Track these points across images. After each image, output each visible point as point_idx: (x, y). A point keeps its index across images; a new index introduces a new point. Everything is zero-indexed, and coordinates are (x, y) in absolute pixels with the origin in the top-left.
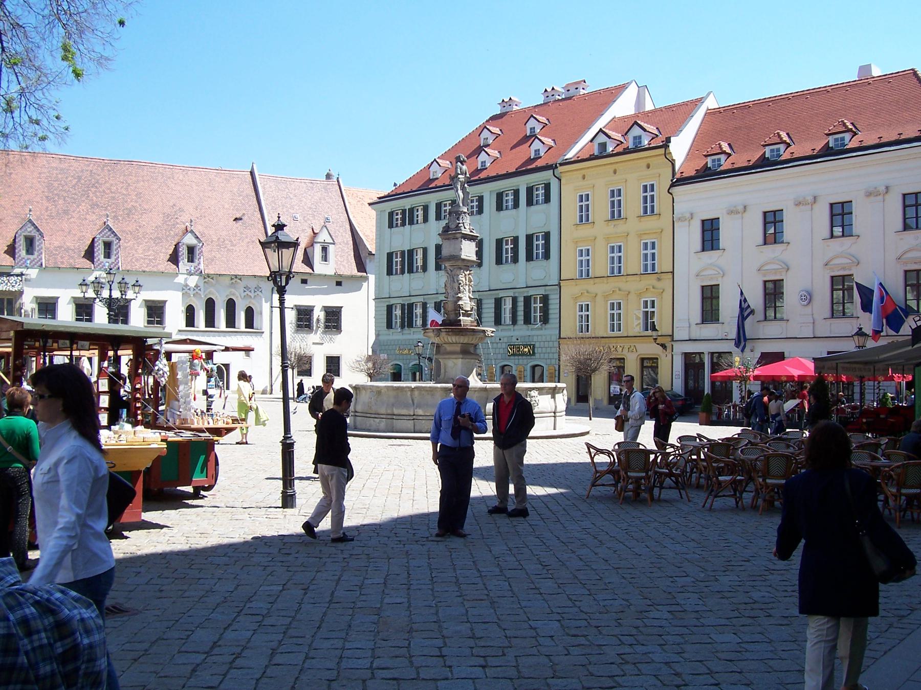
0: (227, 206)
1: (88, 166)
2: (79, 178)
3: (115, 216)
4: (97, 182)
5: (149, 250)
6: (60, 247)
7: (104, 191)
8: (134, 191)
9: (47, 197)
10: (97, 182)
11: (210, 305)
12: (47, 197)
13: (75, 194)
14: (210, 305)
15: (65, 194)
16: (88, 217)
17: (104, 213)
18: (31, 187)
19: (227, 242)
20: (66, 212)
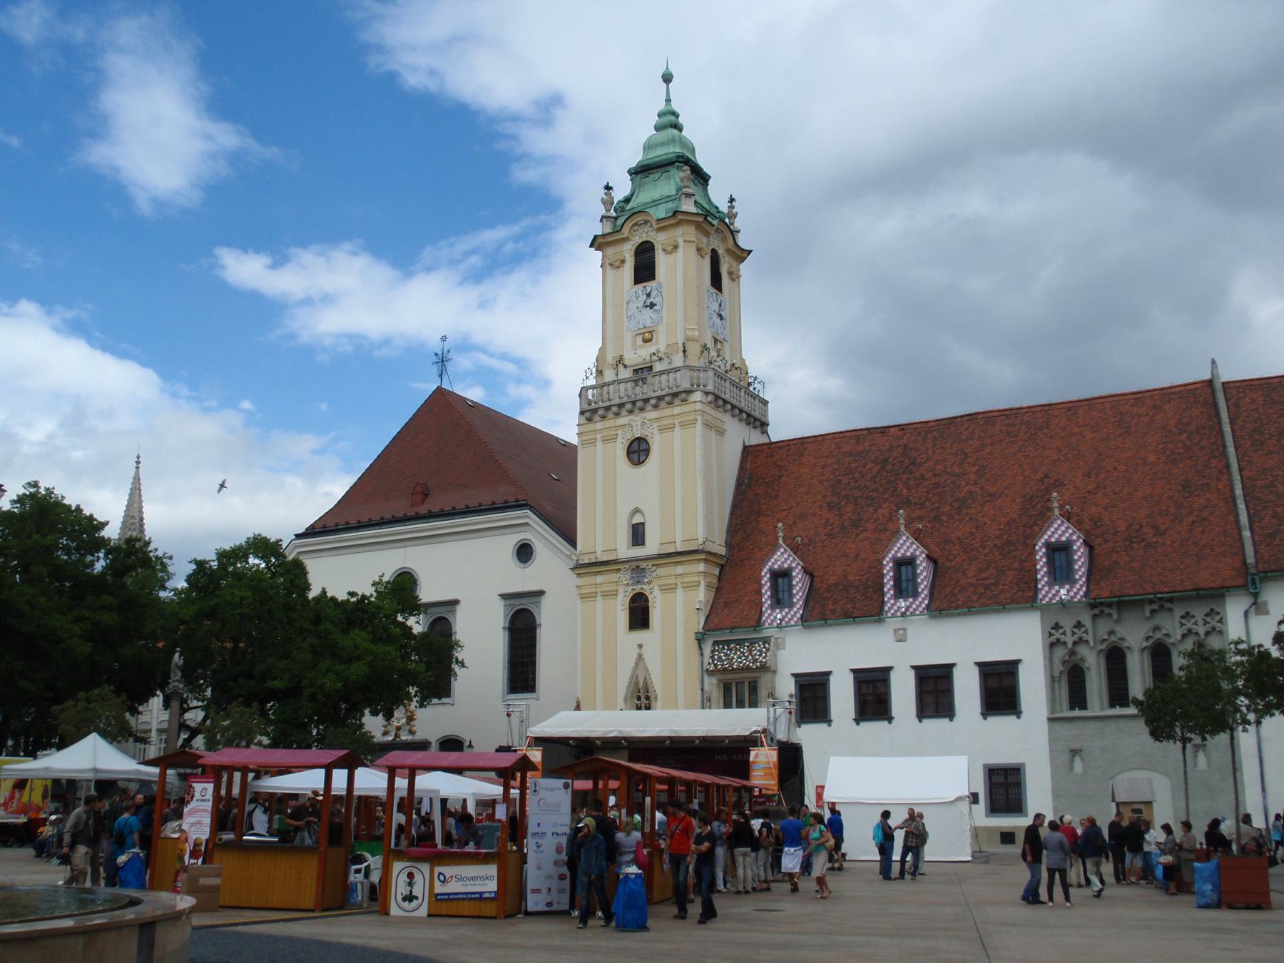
0: (1152, 458)
1: (902, 437)
2: (885, 461)
3: (936, 517)
4: (913, 463)
5: (988, 568)
6: (836, 585)
7: (922, 476)
8: (973, 465)
9: (828, 504)
10: (913, 463)
11: (1115, 659)
12: (828, 504)
13: (873, 491)
14: (1115, 659)
15: (857, 493)
16: (890, 525)
17: (917, 513)
18: (807, 493)
19: (1146, 530)
20: (856, 524)
